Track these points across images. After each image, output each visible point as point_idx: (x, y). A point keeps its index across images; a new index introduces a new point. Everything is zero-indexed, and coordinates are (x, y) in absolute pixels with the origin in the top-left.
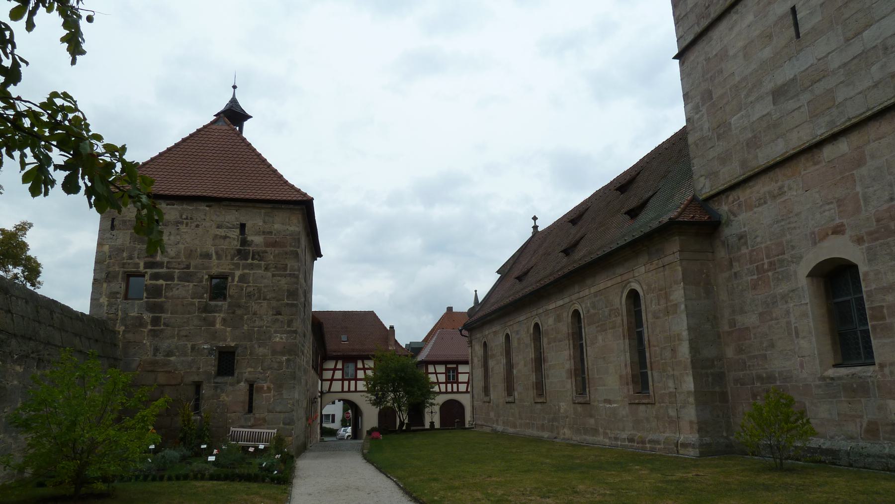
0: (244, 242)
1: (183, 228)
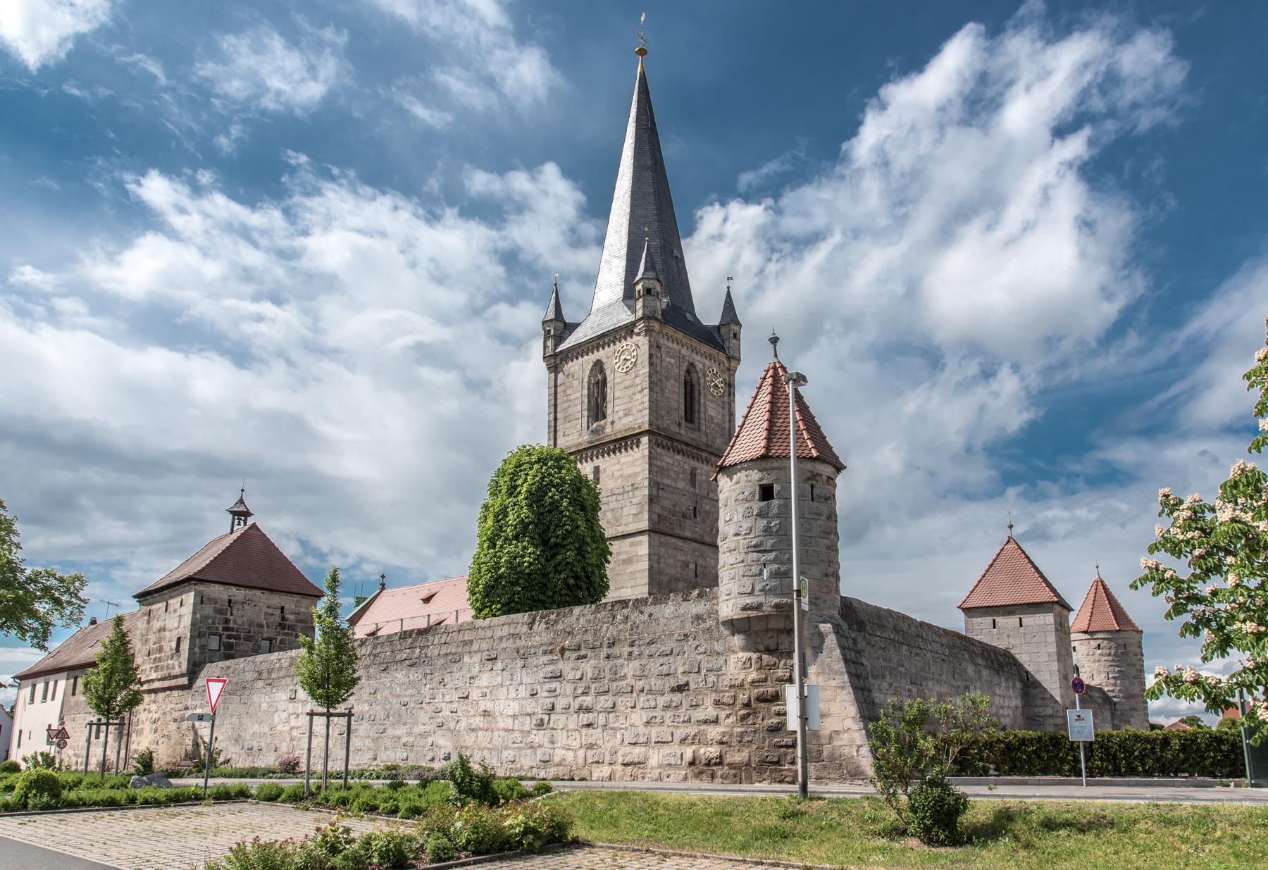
0: (283, 618)
1: (246, 607)
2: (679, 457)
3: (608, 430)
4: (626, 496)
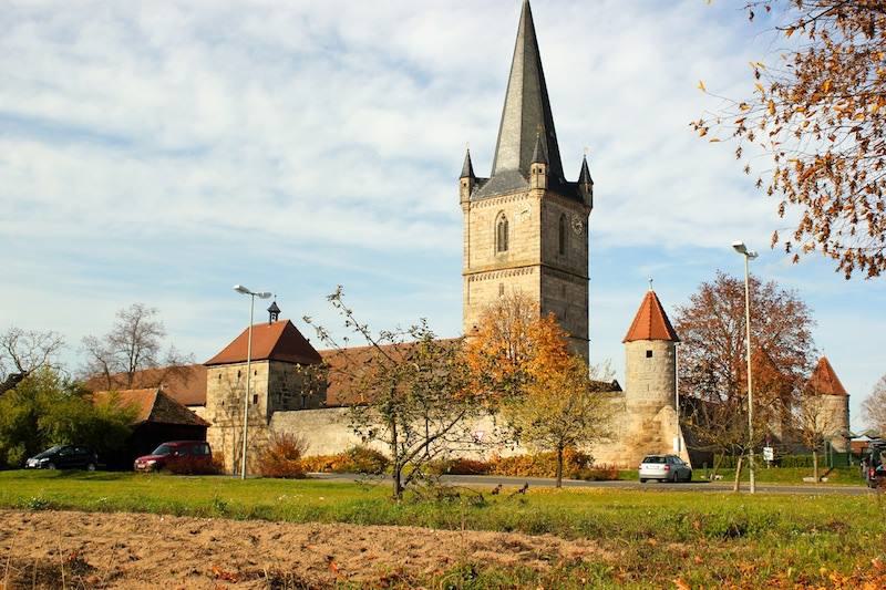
2: (556, 279)
3: (510, 259)
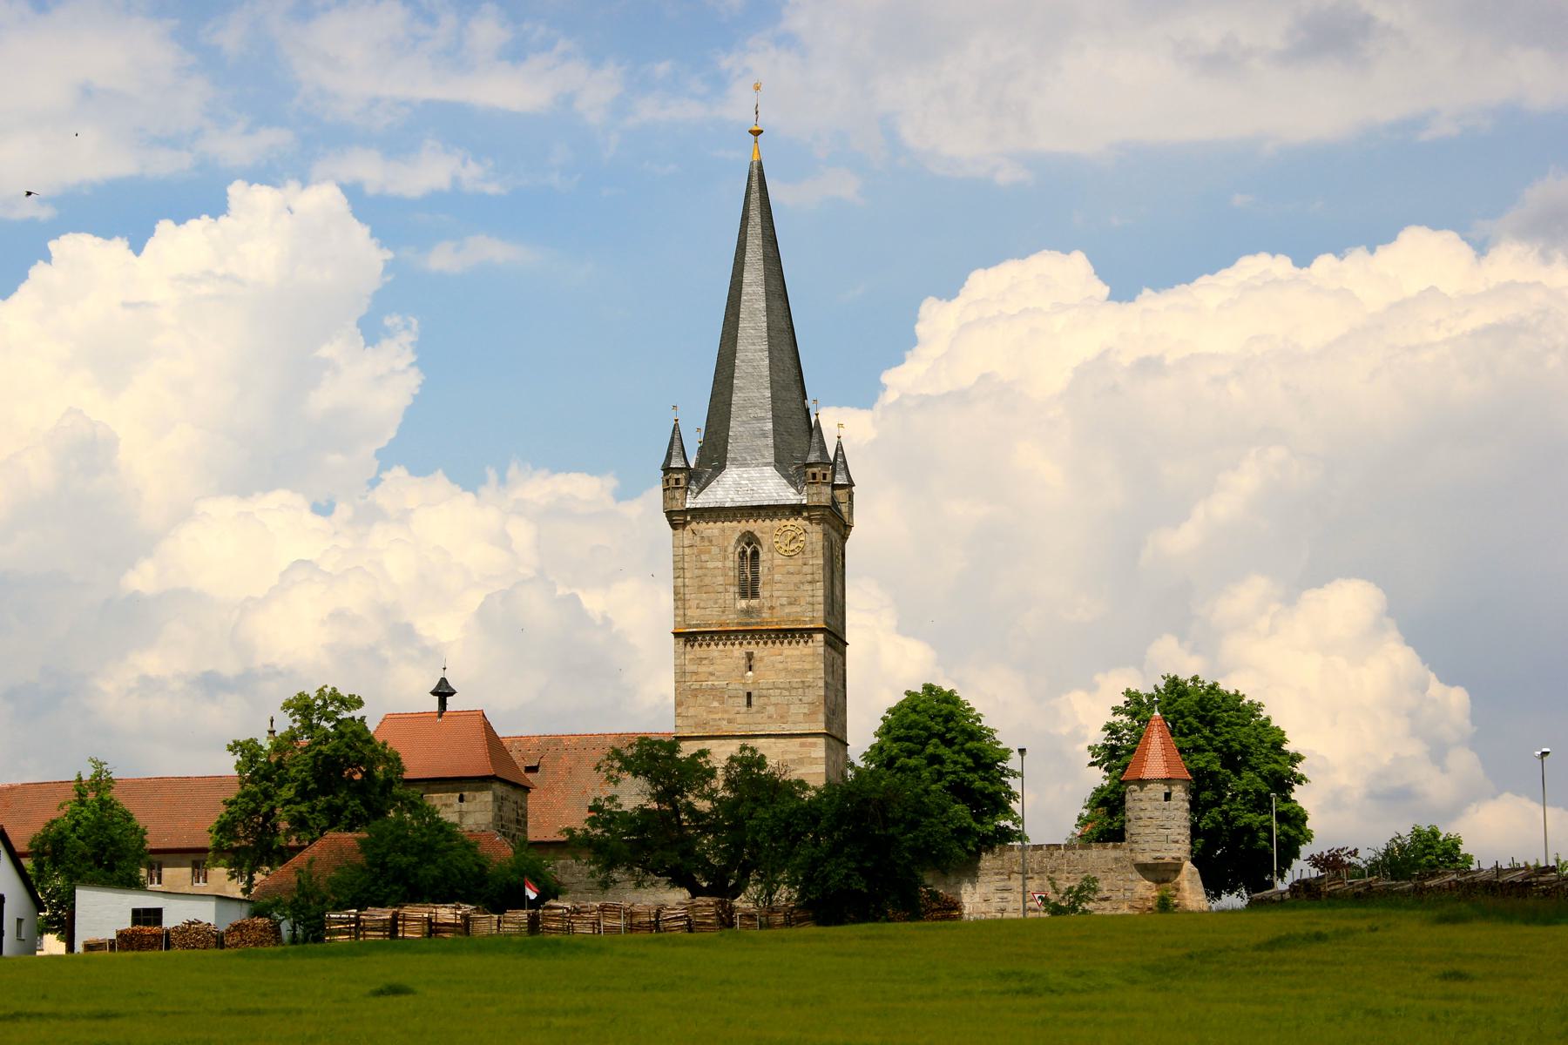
3: (766, 615)
4: (794, 692)
